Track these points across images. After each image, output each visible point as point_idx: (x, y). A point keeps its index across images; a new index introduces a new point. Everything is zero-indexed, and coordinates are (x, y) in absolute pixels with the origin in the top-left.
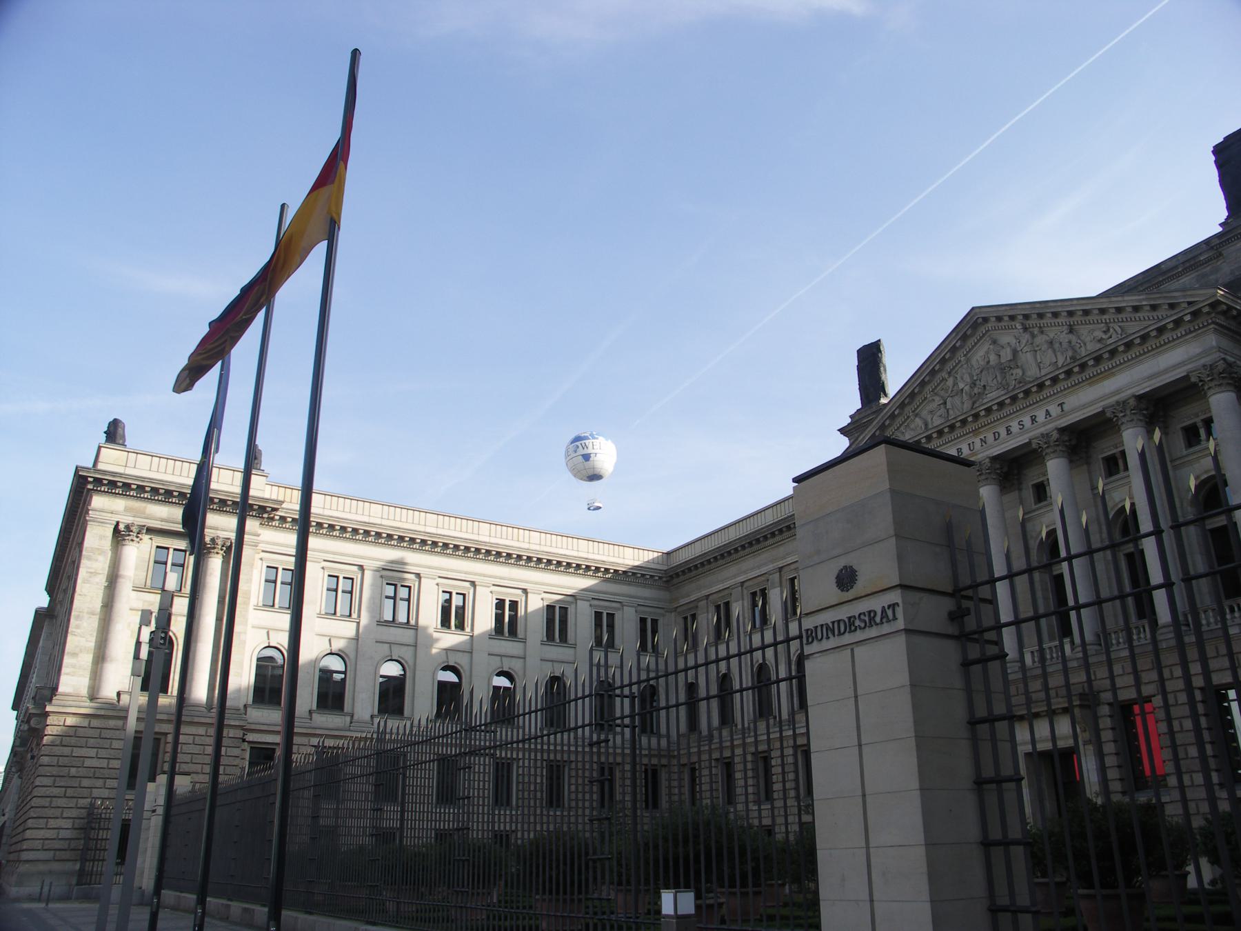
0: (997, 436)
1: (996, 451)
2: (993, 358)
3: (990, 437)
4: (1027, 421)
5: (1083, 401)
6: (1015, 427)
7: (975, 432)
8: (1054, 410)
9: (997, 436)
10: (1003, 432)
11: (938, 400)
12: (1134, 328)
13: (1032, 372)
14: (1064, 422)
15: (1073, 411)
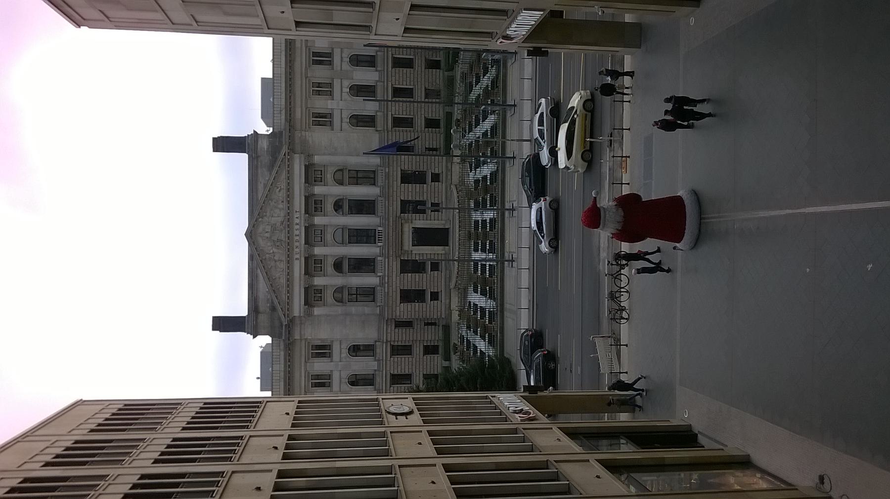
0: (297, 241)
1: (303, 242)
2: (266, 235)
3: (297, 244)
4: (298, 227)
5: (299, 203)
6: (297, 232)
7: (293, 249)
8: (297, 215)
9: (297, 241)
10: (297, 238)
11: (273, 263)
12: (284, 175)
13: (280, 219)
14: (303, 212)
15: (300, 208)
